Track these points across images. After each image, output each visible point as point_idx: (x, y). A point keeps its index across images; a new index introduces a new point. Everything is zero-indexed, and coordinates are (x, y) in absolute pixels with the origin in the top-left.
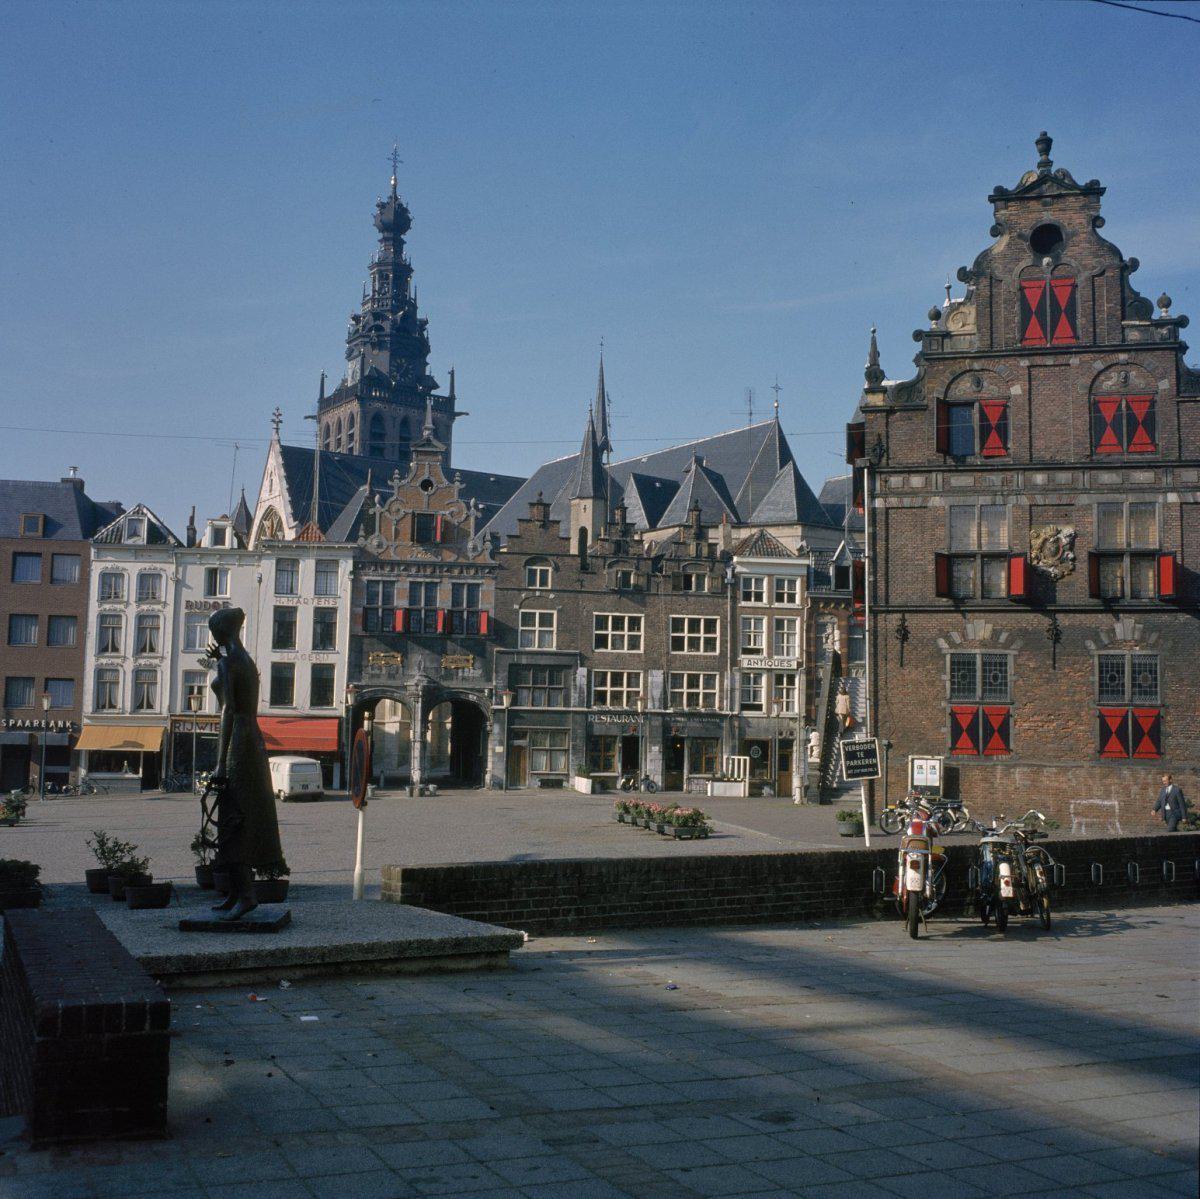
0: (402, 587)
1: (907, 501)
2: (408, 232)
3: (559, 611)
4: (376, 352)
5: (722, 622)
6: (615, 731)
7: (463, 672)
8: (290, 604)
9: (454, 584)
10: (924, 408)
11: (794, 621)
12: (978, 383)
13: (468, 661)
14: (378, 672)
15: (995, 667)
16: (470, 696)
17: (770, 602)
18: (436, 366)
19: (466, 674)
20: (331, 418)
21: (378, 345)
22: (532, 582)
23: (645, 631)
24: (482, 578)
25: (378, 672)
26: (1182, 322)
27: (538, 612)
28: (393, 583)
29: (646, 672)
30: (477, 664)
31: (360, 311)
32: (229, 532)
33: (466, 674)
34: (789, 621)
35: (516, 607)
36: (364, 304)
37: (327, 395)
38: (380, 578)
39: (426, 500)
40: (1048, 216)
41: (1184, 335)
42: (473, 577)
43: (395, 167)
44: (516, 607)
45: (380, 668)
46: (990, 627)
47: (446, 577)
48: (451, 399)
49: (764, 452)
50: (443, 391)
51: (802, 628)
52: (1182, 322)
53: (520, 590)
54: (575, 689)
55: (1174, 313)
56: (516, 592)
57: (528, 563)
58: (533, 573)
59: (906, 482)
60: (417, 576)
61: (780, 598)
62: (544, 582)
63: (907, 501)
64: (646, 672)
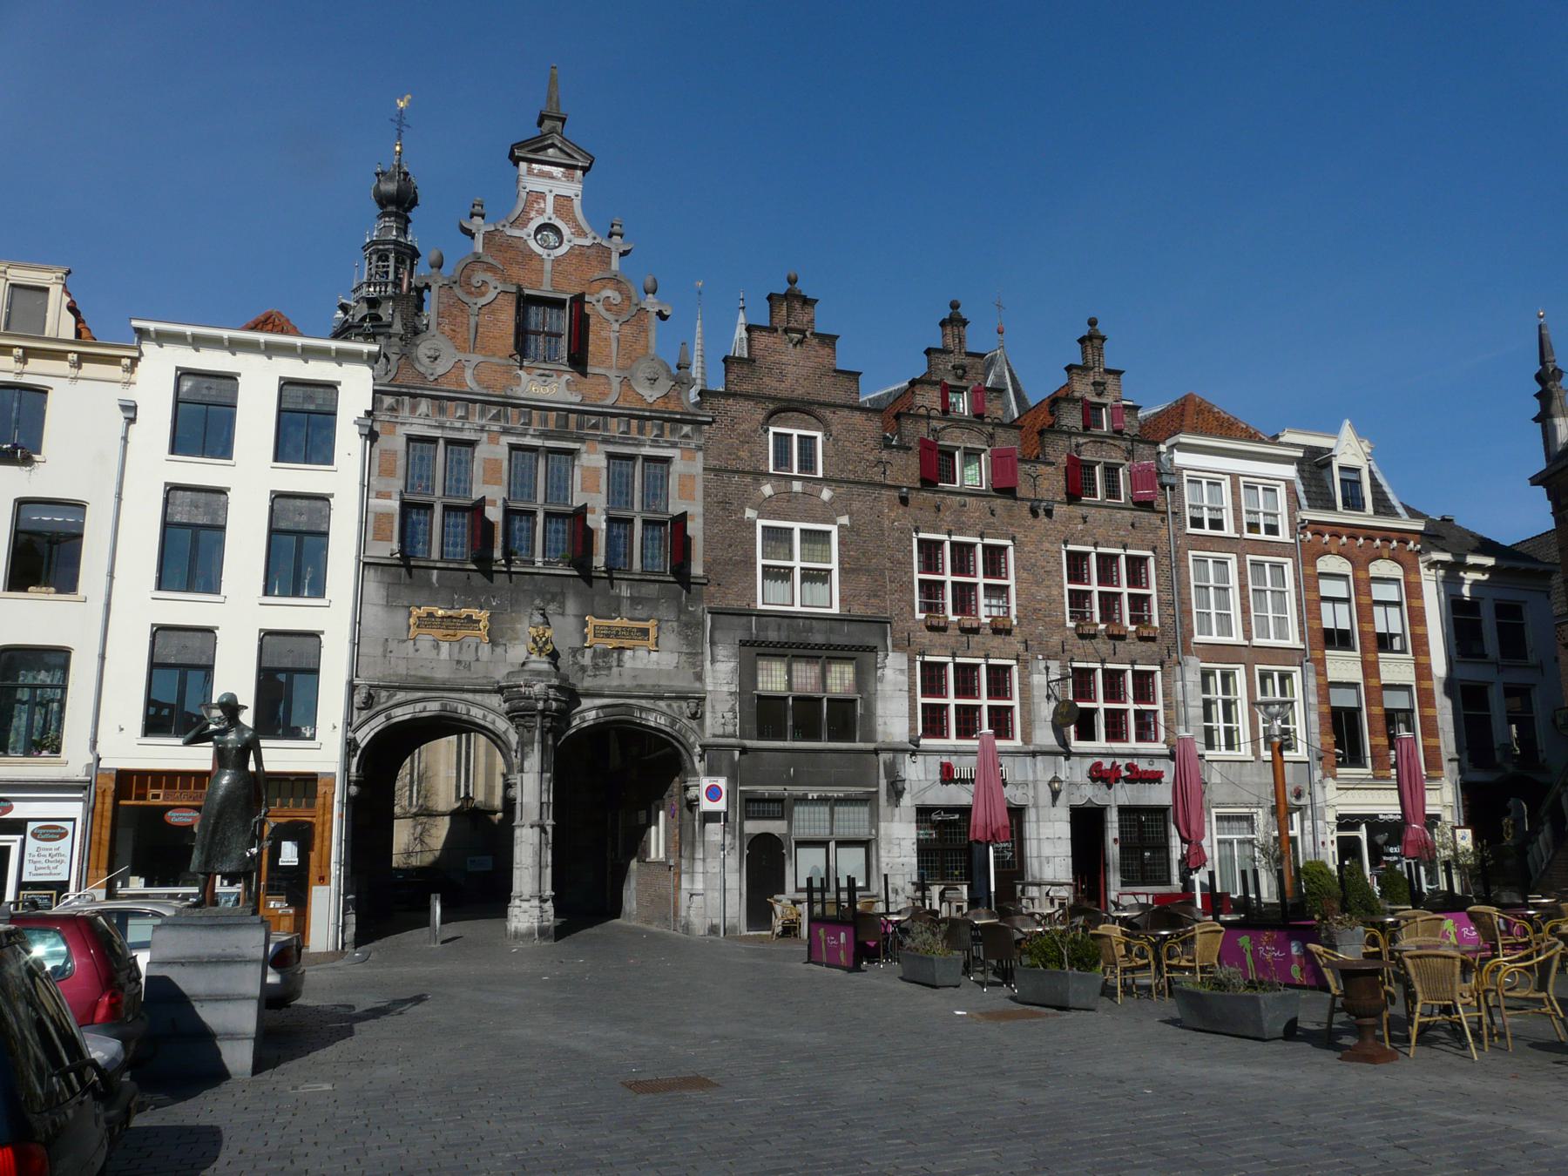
3: (841, 527)
5: (1156, 561)
9: (611, 456)
11: (1280, 566)
13: (645, 632)
17: (1238, 529)
24: (674, 445)
27: (797, 527)
28: (472, 444)
34: (1273, 565)
35: (750, 513)
39: (548, 267)
42: (655, 443)
43: (400, 132)
44: (750, 513)
47: (594, 438)
51: (1297, 581)
53: (760, 475)
57: (771, 418)
58: (783, 441)
60: (525, 435)
61: (1253, 527)
62: (807, 462)
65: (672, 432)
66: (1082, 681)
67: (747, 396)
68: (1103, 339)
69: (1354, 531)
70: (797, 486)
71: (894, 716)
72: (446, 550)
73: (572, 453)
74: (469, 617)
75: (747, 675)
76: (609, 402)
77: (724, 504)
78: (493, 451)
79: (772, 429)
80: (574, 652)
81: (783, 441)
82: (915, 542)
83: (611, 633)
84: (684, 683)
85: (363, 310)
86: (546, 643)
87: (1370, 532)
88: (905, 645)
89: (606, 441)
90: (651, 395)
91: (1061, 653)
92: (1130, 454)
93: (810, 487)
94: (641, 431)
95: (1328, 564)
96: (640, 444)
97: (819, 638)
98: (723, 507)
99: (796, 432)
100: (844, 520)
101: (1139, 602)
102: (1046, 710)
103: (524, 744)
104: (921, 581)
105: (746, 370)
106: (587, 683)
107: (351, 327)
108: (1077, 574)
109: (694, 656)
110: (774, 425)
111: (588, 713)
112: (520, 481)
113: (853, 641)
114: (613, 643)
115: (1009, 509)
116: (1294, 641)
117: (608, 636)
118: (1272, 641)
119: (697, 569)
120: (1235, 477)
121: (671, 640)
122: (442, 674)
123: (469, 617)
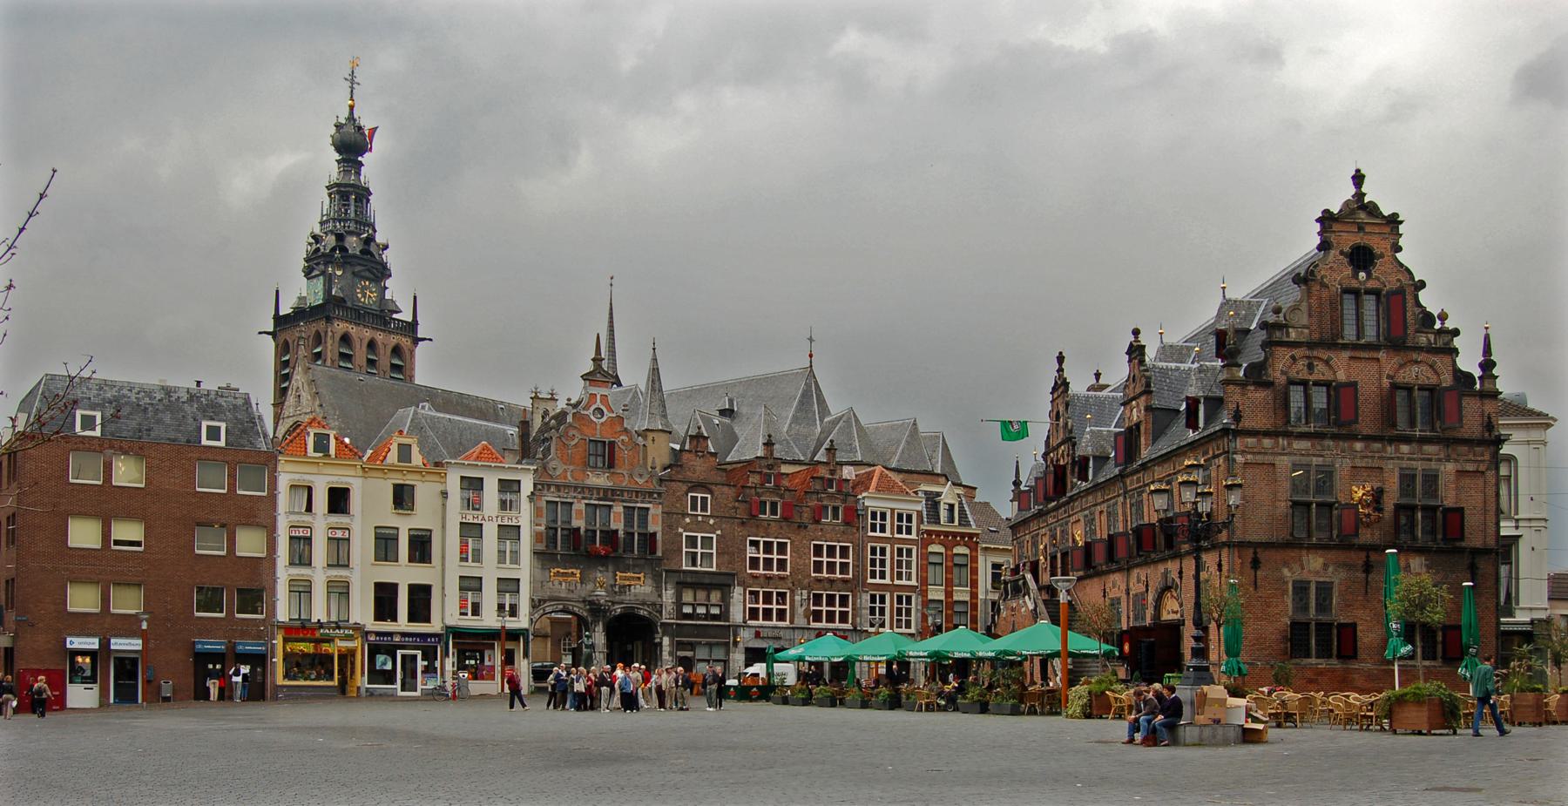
0: (580, 506)
1: (1259, 458)
2: (367, 155)
4: (339, 273)
10: (1269, 385)
12: (1310, 367)
15: (1325, 590)
18: (397, 291)
20: (290, 335)
21: (341, 266)
22: (694, 508)
26: (1456, 332)
27: (699, 535)
29: (793, 592)
31: (317, 231)
32: (415, 450)
36: (322, 223)
37: (285, 310)
40: (1358, 239)
41: (1457, 342)
46: (1321, 560)
48: (413, 325)
49: (803, 395)
50: (406, 316)
52: (1456, 332)
53: (685, 515)
55: (1449, 325)
57: (691, 489)
58: (694, 499)
59: (1397, 450)
61: (900, 531)
62: (704, 508)
63: (1259, 458)
64: (793, 592)
66: (817, 599)
69: (947, 534)
71: (737, 614)
72: (566, 547)
73: (610, 507)
75: (679, 596)
77: (670, 527)
78: (580, 506)
80: (613, 586)
81: (694, 499)
83: (626, 579)
84: (654, 598)
85: (331, 241)
87: (955, 535)
88: (743, 584)
90: (641, 481)
91: (809, 588)
92: (844, 501)
95: (932, 548)
97: (707, 581)
98: (669, 527)
101: (844, 566)
102: (800, 611)
103: (595, 622)
106: (617, 598)
107: (324, 255)
109: (658, 588)
111: (618, 610)
112: (591, 519)
113: (721, 583)
116: (913, 582)
118: (904, 582)
119: (659, 553)
120: (893, 510)
121: (649, 581)
122: (563, 595)
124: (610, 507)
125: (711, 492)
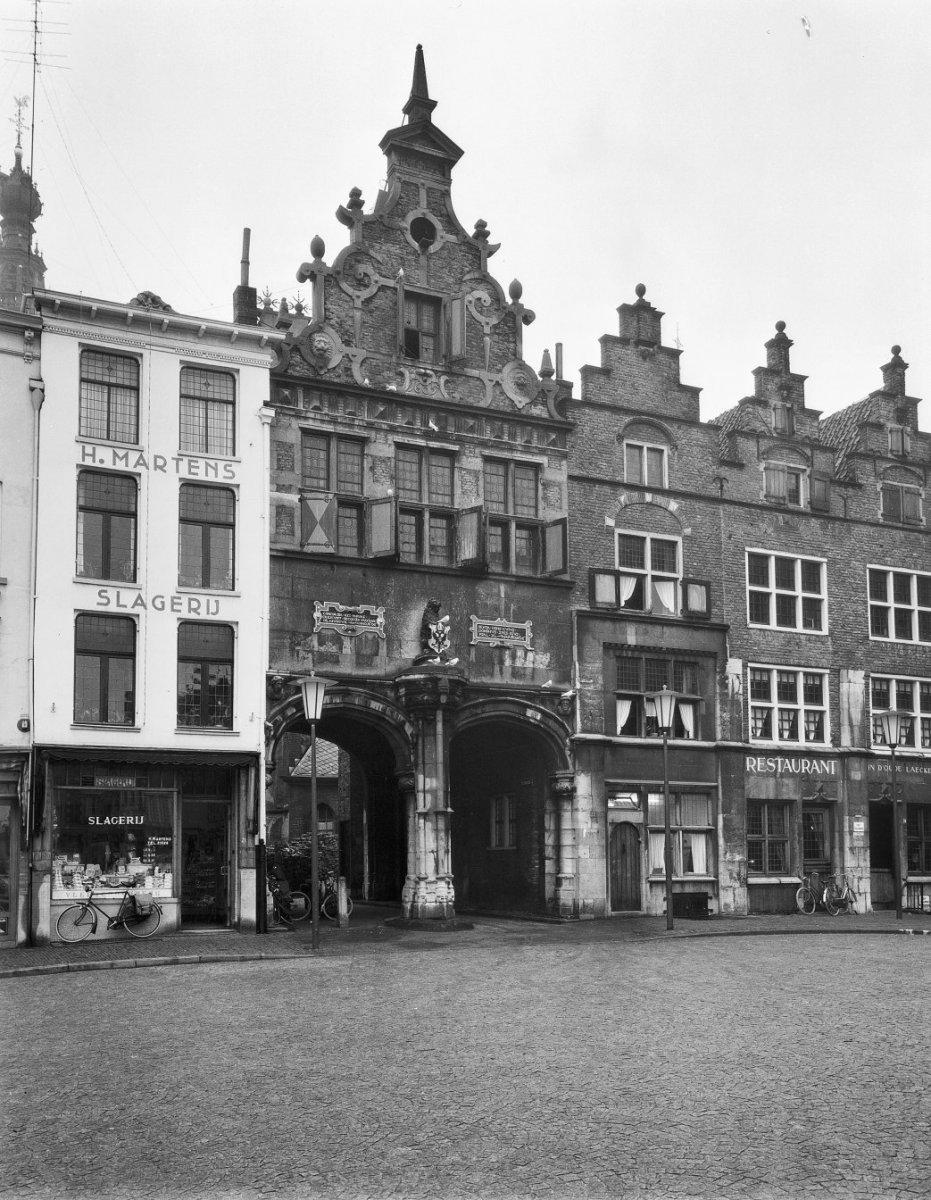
3: (685, 538)
6: (790, 792)
7: (514, 657)
8: (120, 466)
13: (522, 632)
14: (334, 649)
16: (529, 713)
19: (518, 664)
23: (830, 593)
24: (542, 452)
25: (334, 649)
27: (649, 536)
28: (363, 441)
29: (836, 673)
30: (542, 642)
33: (518, 664)
38: (329, 428)
42: (527, 450)
44: (610, 522)
45: (337, 639)
47: (471, 441)
54: (723, 703)
56: (607, 489)
64: (836, 673)
65: (540, 439)
67: (602, 407)
68: (905, 366)
70: (648, 497)
74: (367, 613)
76: (482, 404)
79: (626, 441)
82: (747, 554)
86: (444, 639)
89: (484, 444)
93: (660, 500)
94: (513, 436)
96: (511, 449)
99: (646, 445)
100: (688, 531)
104: (751, 592)
105: (602, 379)
108: (879, 592)
110: (628, 437)
114: (494, 642)
115: (824, 528)
117: (489, 635)
123: (367, 613)
124: (453, 456)
125: (669, 439)
